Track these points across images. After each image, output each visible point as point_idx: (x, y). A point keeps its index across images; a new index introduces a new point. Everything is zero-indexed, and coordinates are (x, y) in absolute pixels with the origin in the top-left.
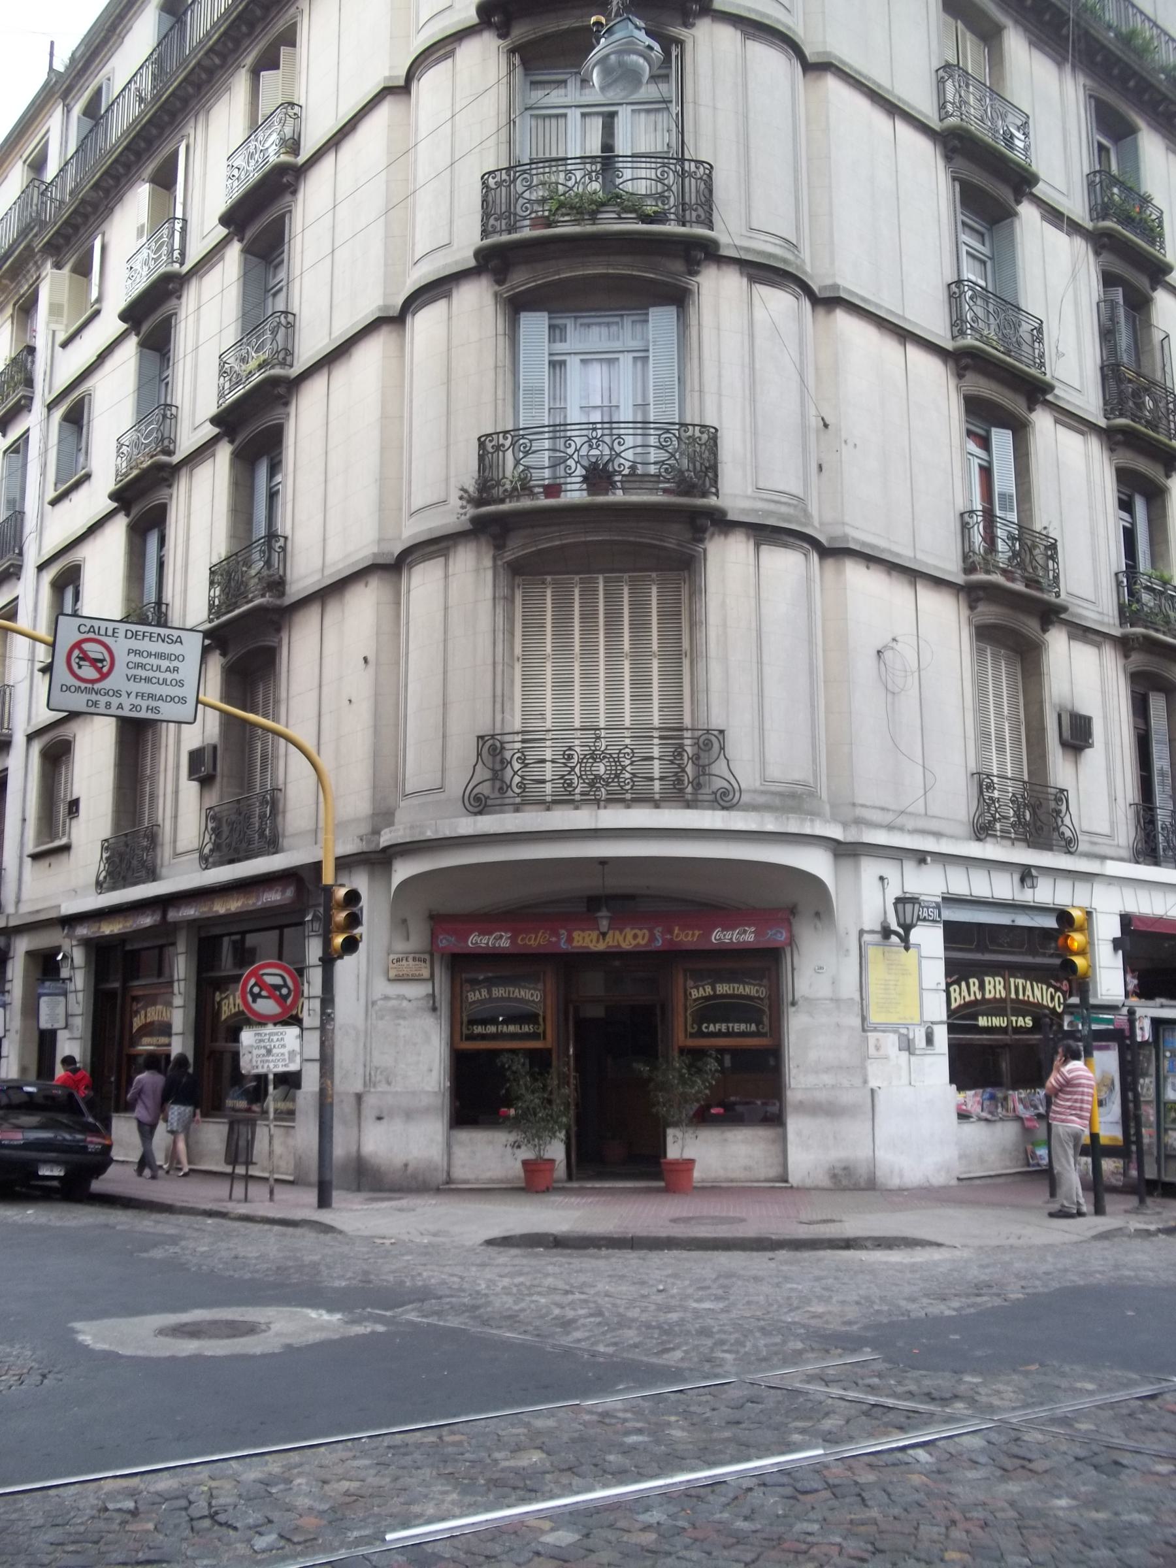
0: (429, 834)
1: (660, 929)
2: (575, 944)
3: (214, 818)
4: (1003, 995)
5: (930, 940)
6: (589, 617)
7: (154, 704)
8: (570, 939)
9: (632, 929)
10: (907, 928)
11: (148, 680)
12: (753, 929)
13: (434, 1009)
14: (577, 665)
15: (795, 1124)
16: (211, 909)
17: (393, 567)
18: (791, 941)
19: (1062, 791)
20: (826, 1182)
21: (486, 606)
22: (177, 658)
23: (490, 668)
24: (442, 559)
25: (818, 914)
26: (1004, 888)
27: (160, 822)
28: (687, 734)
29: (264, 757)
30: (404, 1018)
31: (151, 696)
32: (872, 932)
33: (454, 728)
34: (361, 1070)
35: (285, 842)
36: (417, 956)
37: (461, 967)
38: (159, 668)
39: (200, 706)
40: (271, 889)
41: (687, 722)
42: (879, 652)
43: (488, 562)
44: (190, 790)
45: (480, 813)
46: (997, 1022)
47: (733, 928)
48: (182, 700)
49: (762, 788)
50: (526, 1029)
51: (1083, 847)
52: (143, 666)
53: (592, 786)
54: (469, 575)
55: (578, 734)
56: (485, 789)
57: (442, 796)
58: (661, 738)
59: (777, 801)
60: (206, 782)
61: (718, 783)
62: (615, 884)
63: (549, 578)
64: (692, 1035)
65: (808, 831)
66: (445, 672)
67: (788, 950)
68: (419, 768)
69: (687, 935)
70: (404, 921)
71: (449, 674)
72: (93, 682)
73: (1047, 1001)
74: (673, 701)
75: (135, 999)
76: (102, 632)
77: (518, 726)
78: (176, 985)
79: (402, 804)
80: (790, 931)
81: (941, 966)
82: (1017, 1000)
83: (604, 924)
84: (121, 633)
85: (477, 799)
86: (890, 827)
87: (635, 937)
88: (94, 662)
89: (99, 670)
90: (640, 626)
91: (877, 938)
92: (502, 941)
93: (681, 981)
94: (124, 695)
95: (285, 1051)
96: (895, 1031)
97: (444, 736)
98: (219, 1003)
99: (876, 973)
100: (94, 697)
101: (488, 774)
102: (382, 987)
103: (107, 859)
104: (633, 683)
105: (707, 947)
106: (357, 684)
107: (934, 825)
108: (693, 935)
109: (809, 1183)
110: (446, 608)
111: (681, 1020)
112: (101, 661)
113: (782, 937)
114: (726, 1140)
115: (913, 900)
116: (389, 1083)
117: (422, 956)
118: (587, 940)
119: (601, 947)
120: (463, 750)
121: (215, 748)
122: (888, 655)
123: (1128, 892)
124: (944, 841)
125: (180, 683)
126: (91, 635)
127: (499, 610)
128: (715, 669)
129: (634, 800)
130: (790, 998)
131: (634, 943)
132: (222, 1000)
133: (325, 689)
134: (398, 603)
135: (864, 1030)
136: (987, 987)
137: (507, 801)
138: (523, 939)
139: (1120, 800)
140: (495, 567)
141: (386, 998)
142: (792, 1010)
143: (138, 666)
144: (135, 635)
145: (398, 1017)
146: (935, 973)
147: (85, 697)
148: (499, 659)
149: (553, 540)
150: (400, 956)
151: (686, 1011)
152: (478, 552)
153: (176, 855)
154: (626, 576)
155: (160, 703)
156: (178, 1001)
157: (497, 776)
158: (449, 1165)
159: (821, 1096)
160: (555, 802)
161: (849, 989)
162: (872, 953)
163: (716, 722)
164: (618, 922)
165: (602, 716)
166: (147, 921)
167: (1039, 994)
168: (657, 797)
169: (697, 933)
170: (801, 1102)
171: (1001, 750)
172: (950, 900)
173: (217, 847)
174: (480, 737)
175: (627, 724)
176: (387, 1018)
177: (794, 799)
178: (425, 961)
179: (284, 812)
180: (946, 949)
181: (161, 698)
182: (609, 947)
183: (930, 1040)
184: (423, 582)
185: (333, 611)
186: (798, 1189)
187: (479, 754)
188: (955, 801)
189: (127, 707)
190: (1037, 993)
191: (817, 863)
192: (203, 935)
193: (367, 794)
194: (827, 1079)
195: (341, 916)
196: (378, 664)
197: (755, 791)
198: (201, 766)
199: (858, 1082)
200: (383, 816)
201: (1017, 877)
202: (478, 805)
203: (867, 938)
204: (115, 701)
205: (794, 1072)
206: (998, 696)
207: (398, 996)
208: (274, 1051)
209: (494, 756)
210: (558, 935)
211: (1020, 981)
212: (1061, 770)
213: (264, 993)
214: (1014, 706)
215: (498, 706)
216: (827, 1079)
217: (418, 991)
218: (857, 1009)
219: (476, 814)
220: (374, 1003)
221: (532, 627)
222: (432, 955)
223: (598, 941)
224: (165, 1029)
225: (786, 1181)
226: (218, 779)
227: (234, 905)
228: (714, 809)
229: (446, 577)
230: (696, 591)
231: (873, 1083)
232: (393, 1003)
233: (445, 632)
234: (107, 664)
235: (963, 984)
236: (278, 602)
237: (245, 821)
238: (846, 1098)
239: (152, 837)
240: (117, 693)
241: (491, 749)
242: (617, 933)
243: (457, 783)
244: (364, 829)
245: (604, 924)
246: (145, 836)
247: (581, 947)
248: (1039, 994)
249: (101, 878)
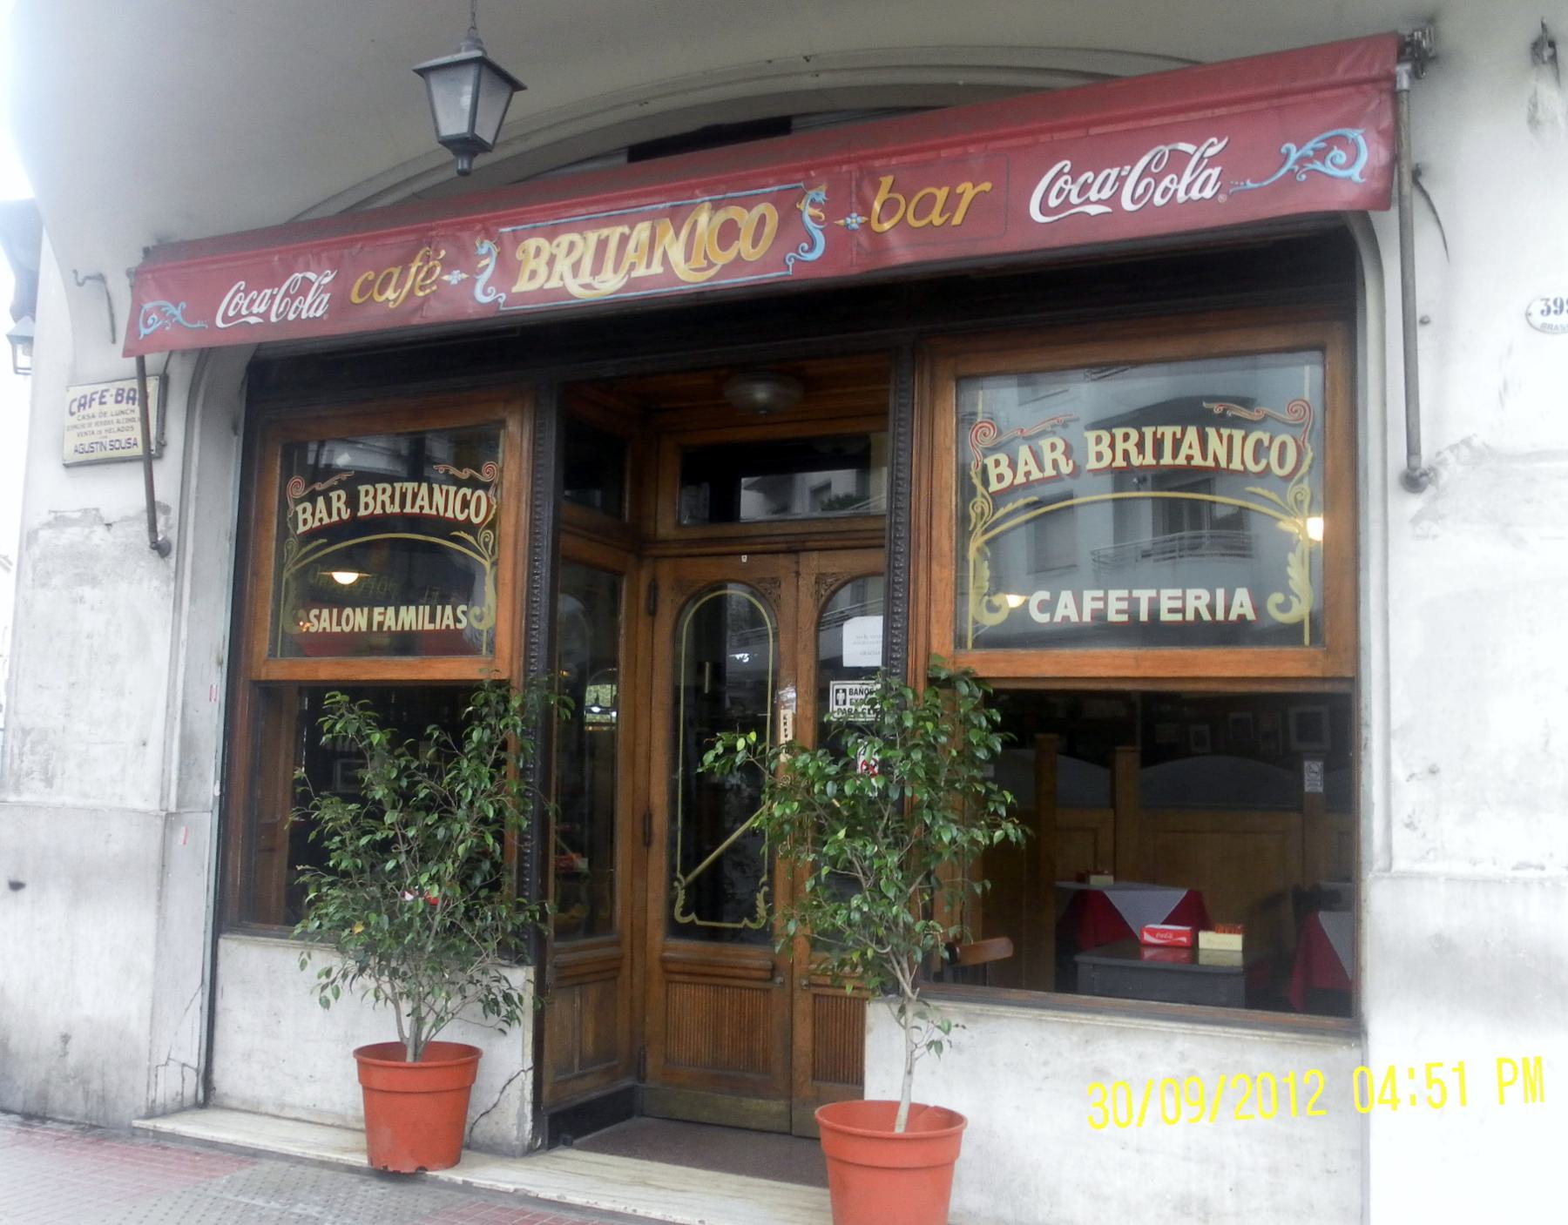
9: (716, 206)
12: (1214, 147)
18: (1402, 180)
30: (94, 582)
67: (1386, 224)
80: (1395, 138)
87: (728, 233)
114: (1101, 1073)
116: (49, 781)
131: (722, 258)
145: (81, 579)
150: (88, 390)
165: (1307, 376)
169: (968, 190)
170: (1443, 945)
176: (57, 580)
217: (121, 494)
223: (597, 270)
232: (73, 534)
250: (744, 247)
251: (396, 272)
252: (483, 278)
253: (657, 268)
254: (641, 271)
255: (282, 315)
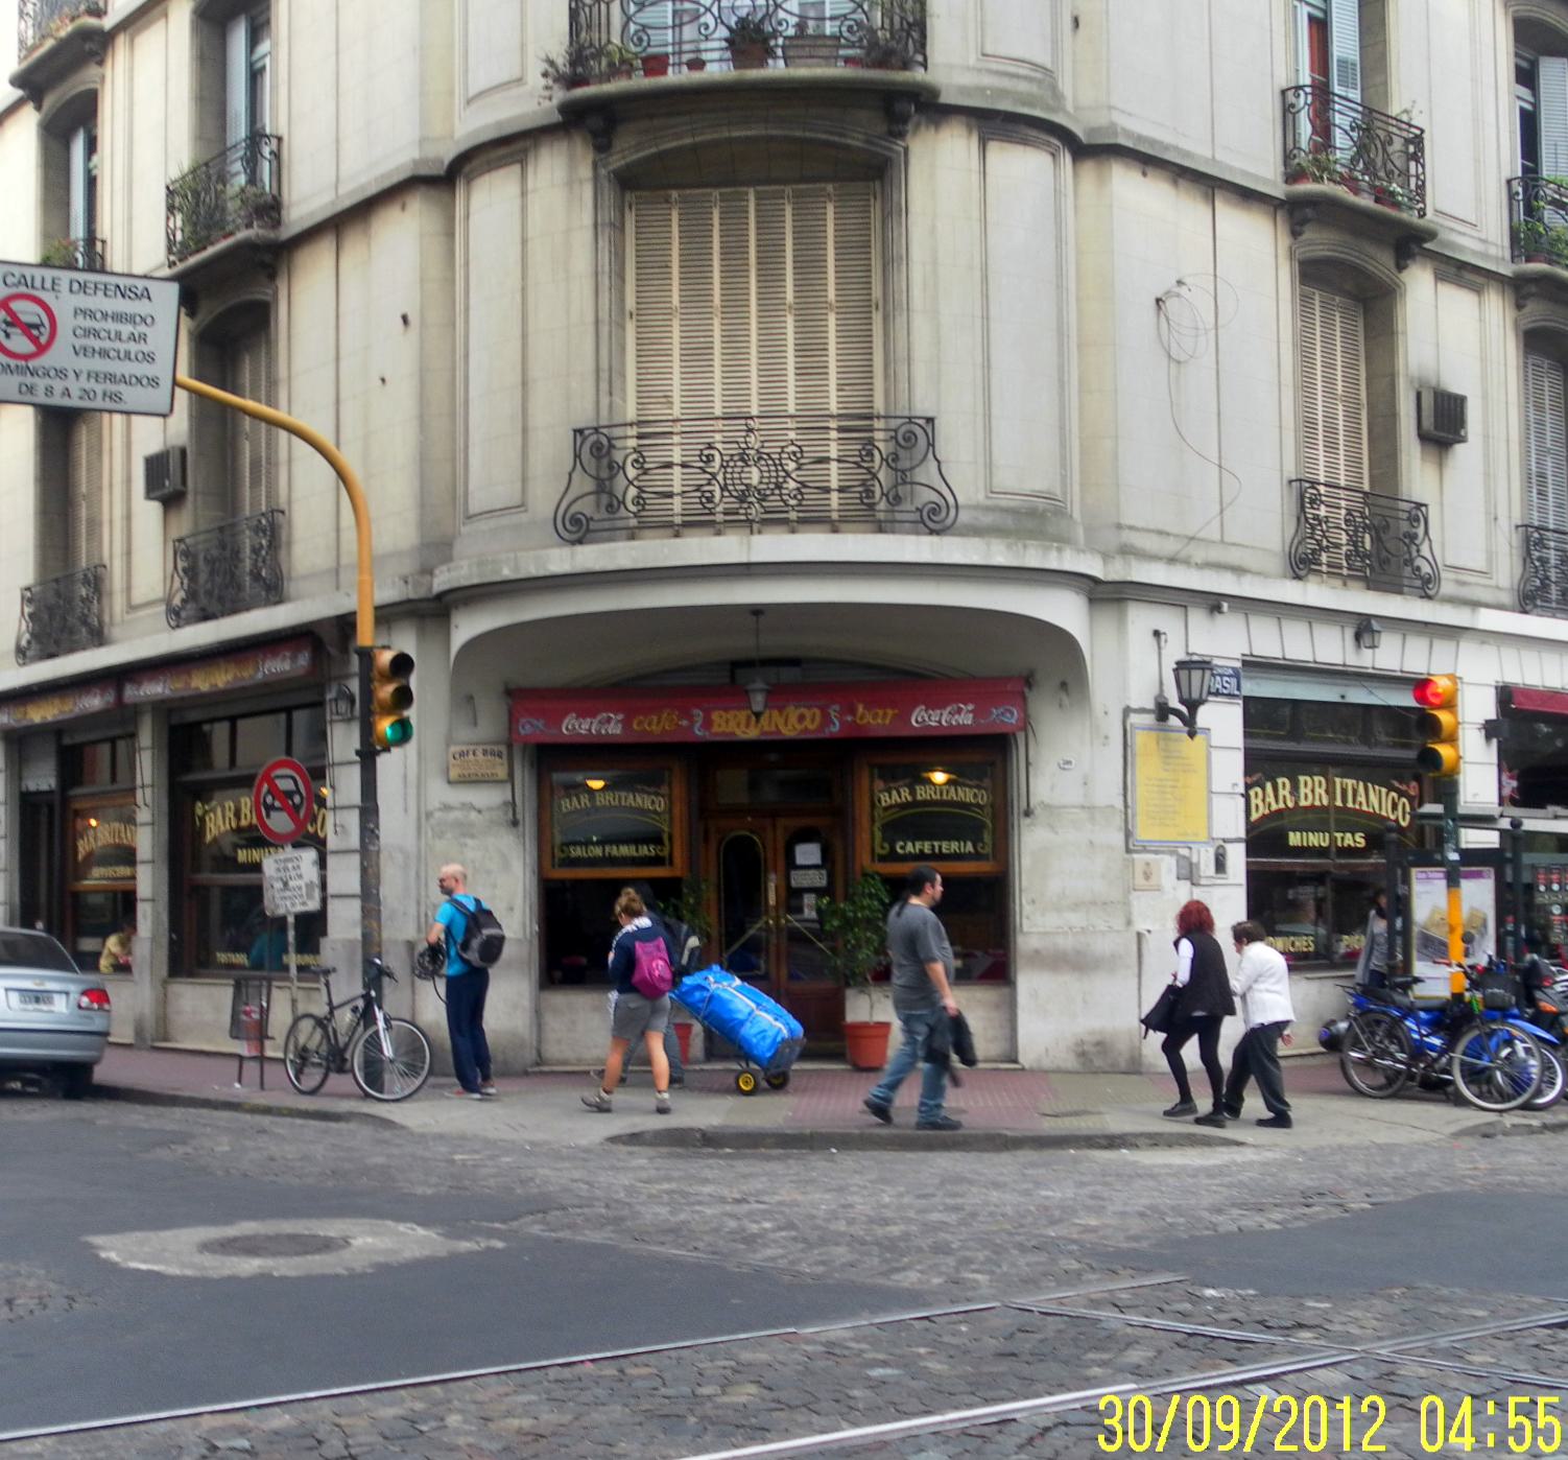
0: (507, 573)
1: (837, 707)
2: (715, 729)
3: (187, 554)
4: (1325, 802)
5: (1223, 722)
6: (734, 252)
7: (113, 388)
8: (707, 724)
10: (1193, 705)
11: (104, 354)
13: (515, 823)
14: (717, 322)
15: (1028, 983)
16: (188, 684)
17: (444, 181)
18: (1026, 724)
19: (1419, 505)
20: (1070, 1062)
21: (583, 238)
22: (144, 320)
23: (591, 329)
24: (516, 168)
25: (1064, 685)
26: (1332, 647)
27: (106, 561)
28: (878, 424)
29: (255, 465)
30: (472, 836)
31: (111, 378)
32: (1142, 711)
33: (540, 418)
34: (412, 910)
35: (291, 588)
36: (488, 748)
37: (552, 761)
38: (119, 336)
39: (178, 391)
40: (275, 654)
41: (879, 405)
42: (1158, 301)
43: (585, 171)
44: (148, 514)
45: (580, 542)
46: (1316, 840)
47: (942, 706)
48: (154, 382)
49: (989, 503)
50: (644, 851)
51: (1447, 587)
52: (97, 334)
53: (742, 502)
54: (556, 196)
55: (719, 425)
56: (586, 507)
57: (524, 518)
58: (840, 429)
59: (1009, 521)
60: (171, 501)
61: (928, 496)
62: (774, 643)
63: (675, 194)
64: (883, 859)
65: (1053, 564)
66: (524, 336)
67: (1021, 737)
68: (489, 476)
69: (875, 716)
70: (470, 699)
71: (531, 339)
72: (26, 357)
73: (1386, 811)
74: (859, 375)
75: (77, 813)
76: (38, 283)
77: (631, 414)
78: (139, 793)
79: (464, 530)
81: (1238, 760)
82: (1345, 809)
83: (758, 702)
84: (64, 286)
85: (575, 521)
86: (1172, 560)
87: (801, 718)
88: (27, 329)
89: (35, 340)
90: (810, 266)
91: (1149, 719)
92: (609, 726)
93: (865, 782)
94: (71, 375)
95: (301, 883)
96: (1172, 853)
97: (525, 431)
98: (202, 820)
99: (1147, 768)
100: (29, 380)
101: (589, 485)
102: (439, 793)
103: (31, 616)
104: (801, 350)
105: (905, 733)
106: (397, 354)
107: (1233, 556)
108: (885, 715)
109: (1047, 1064)
110: (524, 242)
111: (866, 836)
112: (37, 327)
113: (1012, 718)
115: (1204, 665)
117: (496, 748)
118: (733, 725)
119: (752, 733)
120: (552, 450)
121: (183, 452)
122: (1171, 305)
123: (1509, 654)
124: (1247, 578)
125: (149, 358)
126: (23, 289)
127: (603, 243)
128: (921, 327)
129: (803, 521)
130: (1024, 805)
131: (799, 727)
132: (206, 812)
133: (343, 364)
134: (450, 234)
135: (1128, 851)
136: (1303, 790)
137: (620, 524)
138: (640, 723)
139: (1503, 522)
140: (596, 178)
141: (447, 808)
142: (1025, 822)
143: (88, 332)
144: (83, 287)
145: (464, 835)
146: (1230, 768)
147: (16, 380)
148: (604, 315)
149: (678, 138)
150: (464, 748)
151: (873, 821)
152: (571, 158)
153: (132, 608)
154: (788, 190)
155: (122, 388)
156: (144, 815)
157: (603, 487)
158: (539, 1041)
159: (1066, 943)
160: (686, 525)
161: (1108, 790)
162: (1141, 740)
163: (922, 407)
164: (779, 695)
166: (94, 702)
167: (1376, 800)
168: (835, 516)
169: (890, 712)
170: (1037, 952)
171: (1331, 446)
172: (1254, 665)
173: (192, 595)
174: (578, 432)
175: (791, 410)
176: (449, 835)
177: (1035, 518)
178: (500, 756)
179: (289, 544)
180: (1247, 735)
181: (124, 380)
182: (764, 733)
183: (1220, 865)
184: (491, 201)
185: (355, 248)
186: (1032, 1071)
187: (577, 456)
188: (1266, 524)
189: (75, 393)
190: (1373, 799)
191: (1063, 610)
192: (175, 720)
193: (411, 516)
194: (1076, 919)
195: (386, 691)
196: (423, 323)
197: (976, 507)
198: (165, 480)
199: (1118, 923)
200: (436, 547)
201: (1350, 633)
202: (577, 530)
203: (1134, 719)
204: (58, 386)
205: (1027, 909)
206: (1329, 366)
207: (463, 805)
208: (292, 884)
209: (598, 458)
210: (690, 718)
211: (1350, 782)
212: (1417, 477)
213: (277, 804)
214: (1351, 381)
215: (604, 386)
216: (1076, 919)
217: (489, 798)
218: (1119, 821)
219: (573, 543)
220: (429, 815)
221: (652, 268)
222: (510, 746)
223: (748, 725)
224: (127, 856)
225: (1015, 1061)
226: (190, 497)
227: (221, 679)
228: (917, 533)
229: (524, 194)
230: (893, 212)
231: (1141, 925)
233: (524, 277)
234: (46, 331)
235: (1269, 786)
236: (271, 235)
237: (229, 553)
238: (1102, 945)
239: (96, 581)
240: (61, 373)
241: (595, 449)
242: (775, 713)
243: (545, 499)
244: (408, 566)
245: (758, 702)
246: (86, 582)
247: (723, 733)
248: (1376, 800)
249: (24, 643)
250: (808, 723)
251: (655, 718)
252: (698, 725)
253: (773, 729)
254: (766, 728)
255: (599, 732)
